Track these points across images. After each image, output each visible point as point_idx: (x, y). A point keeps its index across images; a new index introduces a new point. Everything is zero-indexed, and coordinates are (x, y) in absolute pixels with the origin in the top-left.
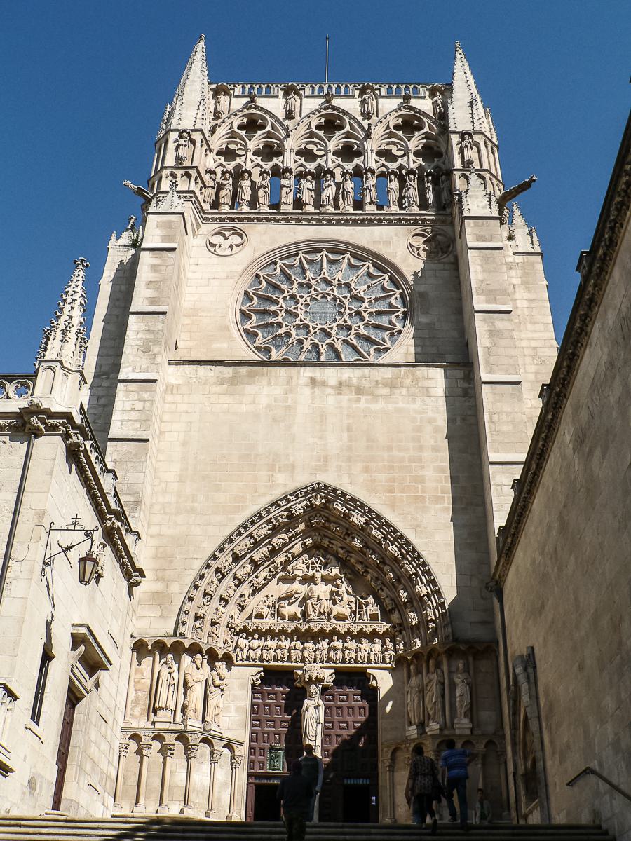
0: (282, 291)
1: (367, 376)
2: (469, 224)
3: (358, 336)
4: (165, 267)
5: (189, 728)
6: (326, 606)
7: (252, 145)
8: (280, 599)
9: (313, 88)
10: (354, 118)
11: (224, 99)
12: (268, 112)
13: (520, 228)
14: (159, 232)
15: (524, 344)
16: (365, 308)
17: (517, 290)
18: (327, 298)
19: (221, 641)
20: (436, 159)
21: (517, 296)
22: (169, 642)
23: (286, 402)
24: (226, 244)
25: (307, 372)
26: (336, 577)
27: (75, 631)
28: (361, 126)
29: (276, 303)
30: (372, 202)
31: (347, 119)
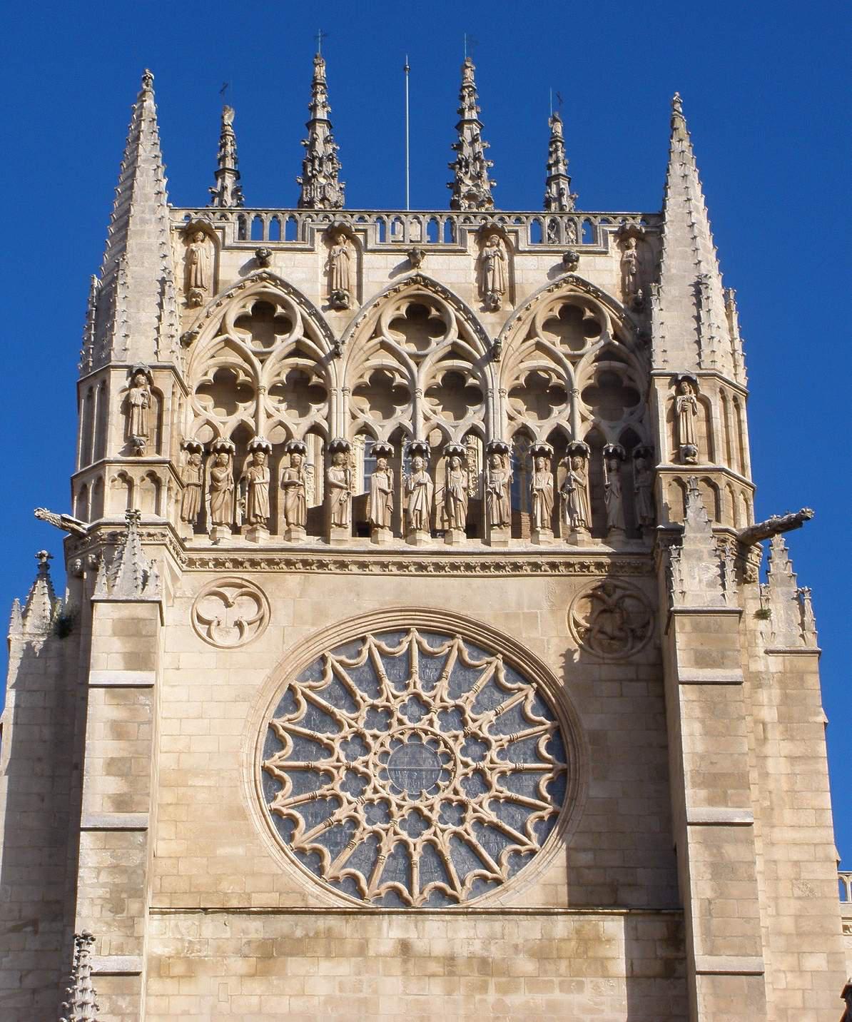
0: (338, 725)
1: (499, 935)
2: (682, 627)
4: (136, 724)
9: (383, 223)
10: (466, 311)
11: (204, 250)
13: (782, 583)
14: (117, 645)
15: (778, 854)
16: (492, 762)
17: (769, 735)
18: (420, 738)
20: (625, 409)
21: (770, 749)
23: (361, 991)
25: (391, 930)
28: (480, 331)
29: (329, 751)
30: (502, 524)
31: (451, 309)
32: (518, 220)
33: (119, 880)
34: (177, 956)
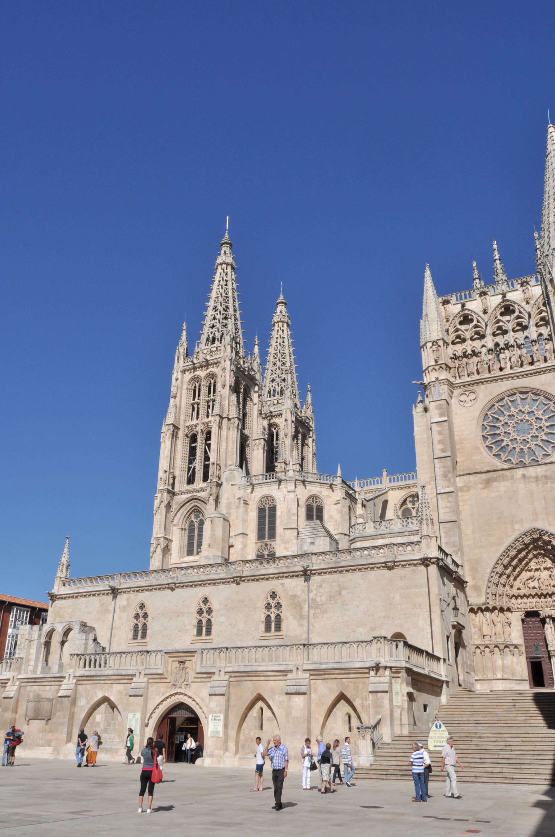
0: (501, 421)
3: (542, 440)
5: (499, 642)
6: (547, 583)
7: (468, 335)
8: (527, 580)
10: (519, 305)
12: (472, 311)
14: (437, 412)
19: (505, 603)
22: (483, 607)
24: (468, 399)
25: (520, 472)
26: (550, 568)
27: (453, 624)
28: (524, 310)
30: (539, 361)
31: (516, 306)
32: (531, 277)
33: (446, 469)
34: (465, 486)
